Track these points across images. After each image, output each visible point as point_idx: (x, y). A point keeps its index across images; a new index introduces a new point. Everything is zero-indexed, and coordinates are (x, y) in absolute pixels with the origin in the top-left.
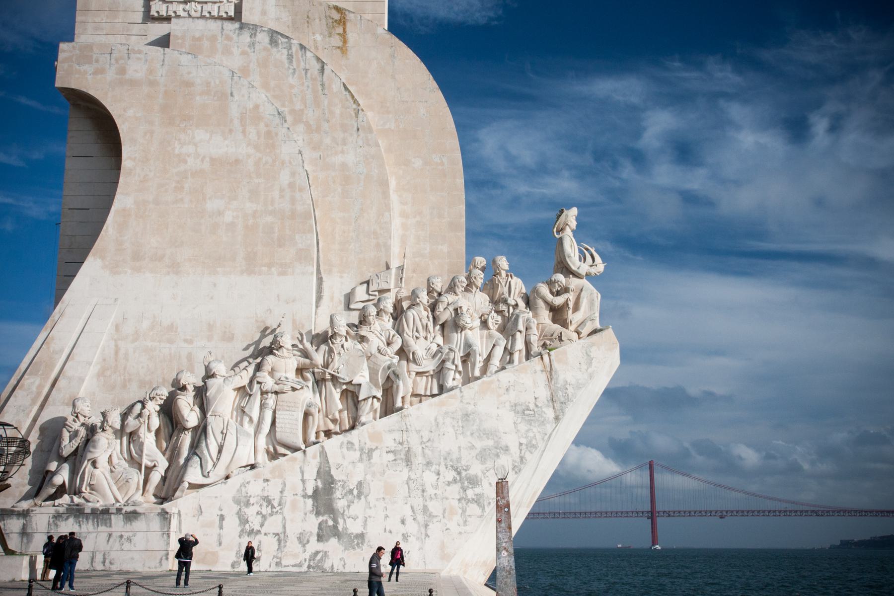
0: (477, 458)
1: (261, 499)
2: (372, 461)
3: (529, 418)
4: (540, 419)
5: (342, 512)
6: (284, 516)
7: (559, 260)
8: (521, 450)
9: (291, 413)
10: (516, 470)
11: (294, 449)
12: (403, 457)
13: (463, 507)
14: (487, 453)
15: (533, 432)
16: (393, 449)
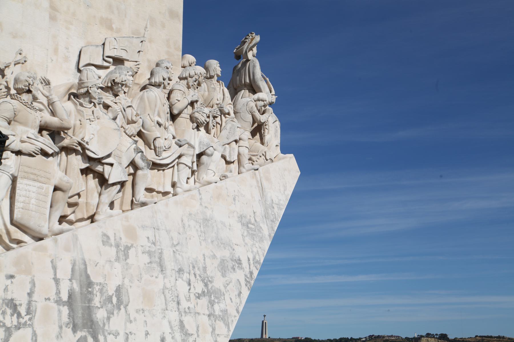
0: (219, 270)
1: (3, 303)
2: (128, 261)
3: (252, 232)
4: (259, 235)
5: (102, 325)
6: (35, 329)
7: (248, 81)
8: (250, 266)
9: (39, 184)
10: (248, 286)
11: (31, 235)
12: (157, 260)
13: (212, 324)
14: (226, 265)
15: (257, 248)
16: (147, 249)
